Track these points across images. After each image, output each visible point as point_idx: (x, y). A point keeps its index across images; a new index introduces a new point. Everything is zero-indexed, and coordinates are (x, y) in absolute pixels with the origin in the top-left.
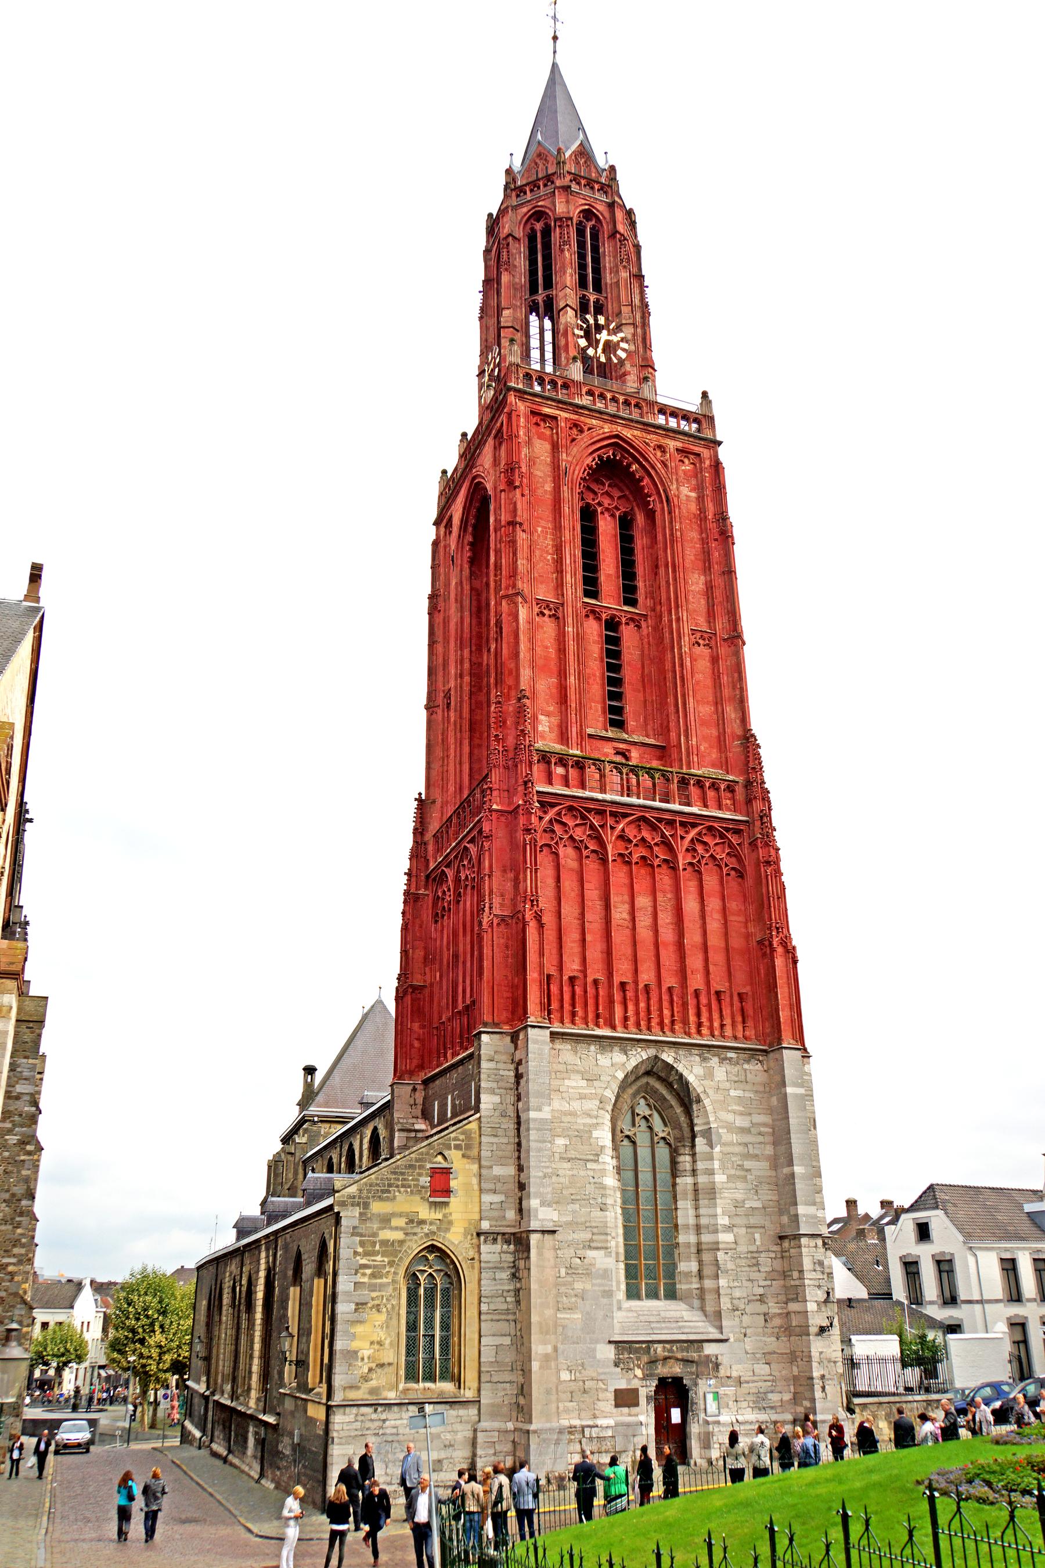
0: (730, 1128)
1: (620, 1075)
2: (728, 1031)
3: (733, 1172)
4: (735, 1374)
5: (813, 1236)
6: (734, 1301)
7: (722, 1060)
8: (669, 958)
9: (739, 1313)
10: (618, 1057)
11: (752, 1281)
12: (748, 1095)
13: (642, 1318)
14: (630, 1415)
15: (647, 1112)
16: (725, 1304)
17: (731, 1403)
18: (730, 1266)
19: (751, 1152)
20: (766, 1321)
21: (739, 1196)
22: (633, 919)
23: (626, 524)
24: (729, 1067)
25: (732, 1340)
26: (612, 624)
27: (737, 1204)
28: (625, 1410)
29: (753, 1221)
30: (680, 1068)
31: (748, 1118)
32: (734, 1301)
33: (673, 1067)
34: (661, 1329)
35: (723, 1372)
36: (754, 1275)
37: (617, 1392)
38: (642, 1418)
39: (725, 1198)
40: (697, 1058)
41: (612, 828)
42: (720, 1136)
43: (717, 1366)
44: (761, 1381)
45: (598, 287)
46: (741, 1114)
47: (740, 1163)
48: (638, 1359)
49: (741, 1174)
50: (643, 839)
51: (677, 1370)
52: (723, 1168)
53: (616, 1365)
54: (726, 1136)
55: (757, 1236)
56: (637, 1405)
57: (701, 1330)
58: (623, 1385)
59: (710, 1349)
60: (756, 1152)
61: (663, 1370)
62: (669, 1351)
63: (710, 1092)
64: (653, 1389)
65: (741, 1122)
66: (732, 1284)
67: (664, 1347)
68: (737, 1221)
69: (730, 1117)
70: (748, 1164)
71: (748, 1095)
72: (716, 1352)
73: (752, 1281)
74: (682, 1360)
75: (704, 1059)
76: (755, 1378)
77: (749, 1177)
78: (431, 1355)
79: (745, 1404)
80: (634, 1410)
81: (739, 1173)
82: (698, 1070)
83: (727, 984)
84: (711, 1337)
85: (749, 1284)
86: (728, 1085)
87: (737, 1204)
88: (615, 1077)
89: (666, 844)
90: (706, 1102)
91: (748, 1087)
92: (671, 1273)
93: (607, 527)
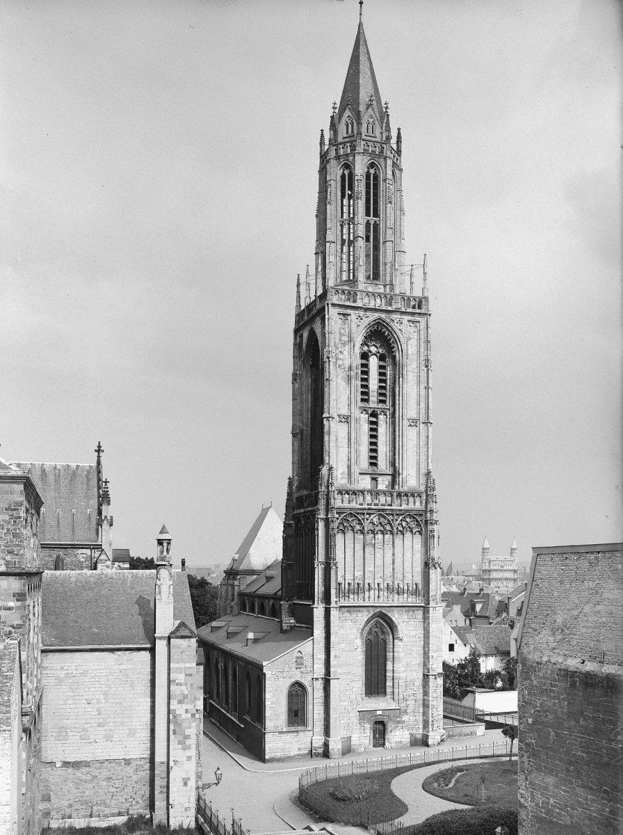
5: (433, 675)
8: (389, 571)
15: (377, 630)
16: (401, 696)
23: (382, 358)
26: (374, 414)
33: (385, 615)
41: (367, 519)
45: (376, 215)
50: (380, 523)
54: (405, 639)
65: (413, 633)
78: (297, 715)
82: (396, 615)
89: (391, 525)
90: (399, 627)
93: (374, 362)
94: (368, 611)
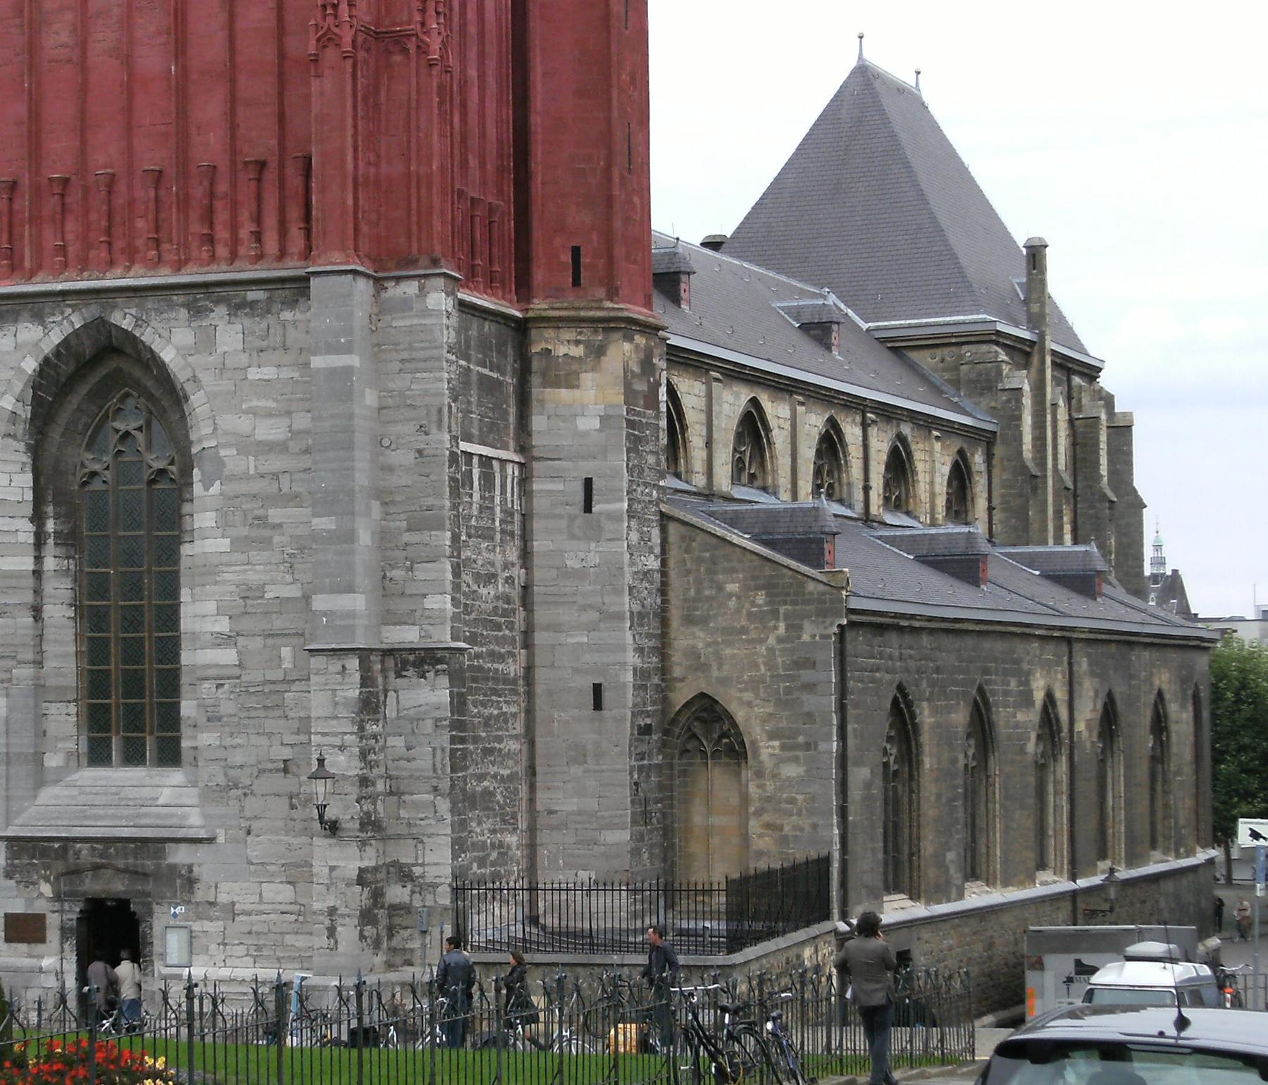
0: (247, 445)
1: (30, 365)
2: (271, 243)
3: (244, 531)
4: (223, 898)
6: (232, 772)
7: (238, 308)
9: (240, 792)
10: (29, 332)
11: (270, 735)
12: (286, 373)
13: (83, 799)
14: (30, 956)
17: (213, 947)
18: (227, 708)
19: (285, 490)
20: (293, 807)
21: (253, 577)
22: (83, 45)
24: (247, 322)
25: (221, 840)
27: (250, 593)
28: (23, 947)
29: (278, 624)
30: (147, 336)
31: (285, 422)
32: (232, 772)
34: (96, 817)
35: (200, 894)
36: (270, 725)
37: (7, 916)
38: (47, 962)
39: (224, 582)
40: (183, 313)
42: (221, 463)
43: (191, 882)
44: (275, 912)
46: (269, 414)
47: (260, 512)
48: (46, 867)
49: (255, 534)
51: (118, 886)
52: (224, 524)
53: (8, 875)
55: (286, 652)
56: (42, 940)
57: (175, 821)
58: (18, 907)
59: (179, 856)
60: (296, 488)
61: (91, 886)
62: (101, 856)
63: (205, 378)
64: (75, 916)
66: (228, 742)
67: (93, 849)
68: (246, 624)
69: (243, 424)
70: (275, 515)
71: (286, 373)
72: (187, 861)
73: (270, 735)
74: (125, 871)
75: (197, 311)
76: (263, 907)
77: (276, 539)
79: (241, 950)
80: (38, 948)
81: (255, 533)
82: (184, 335)
83: (273, 142)
84: (181, 833)
85: (263, 741)
86: (244, 359)
87: (250, 593)
88: (20, 370)
91: (287, 359)
92: (170, 719)
94: (39, 317)
